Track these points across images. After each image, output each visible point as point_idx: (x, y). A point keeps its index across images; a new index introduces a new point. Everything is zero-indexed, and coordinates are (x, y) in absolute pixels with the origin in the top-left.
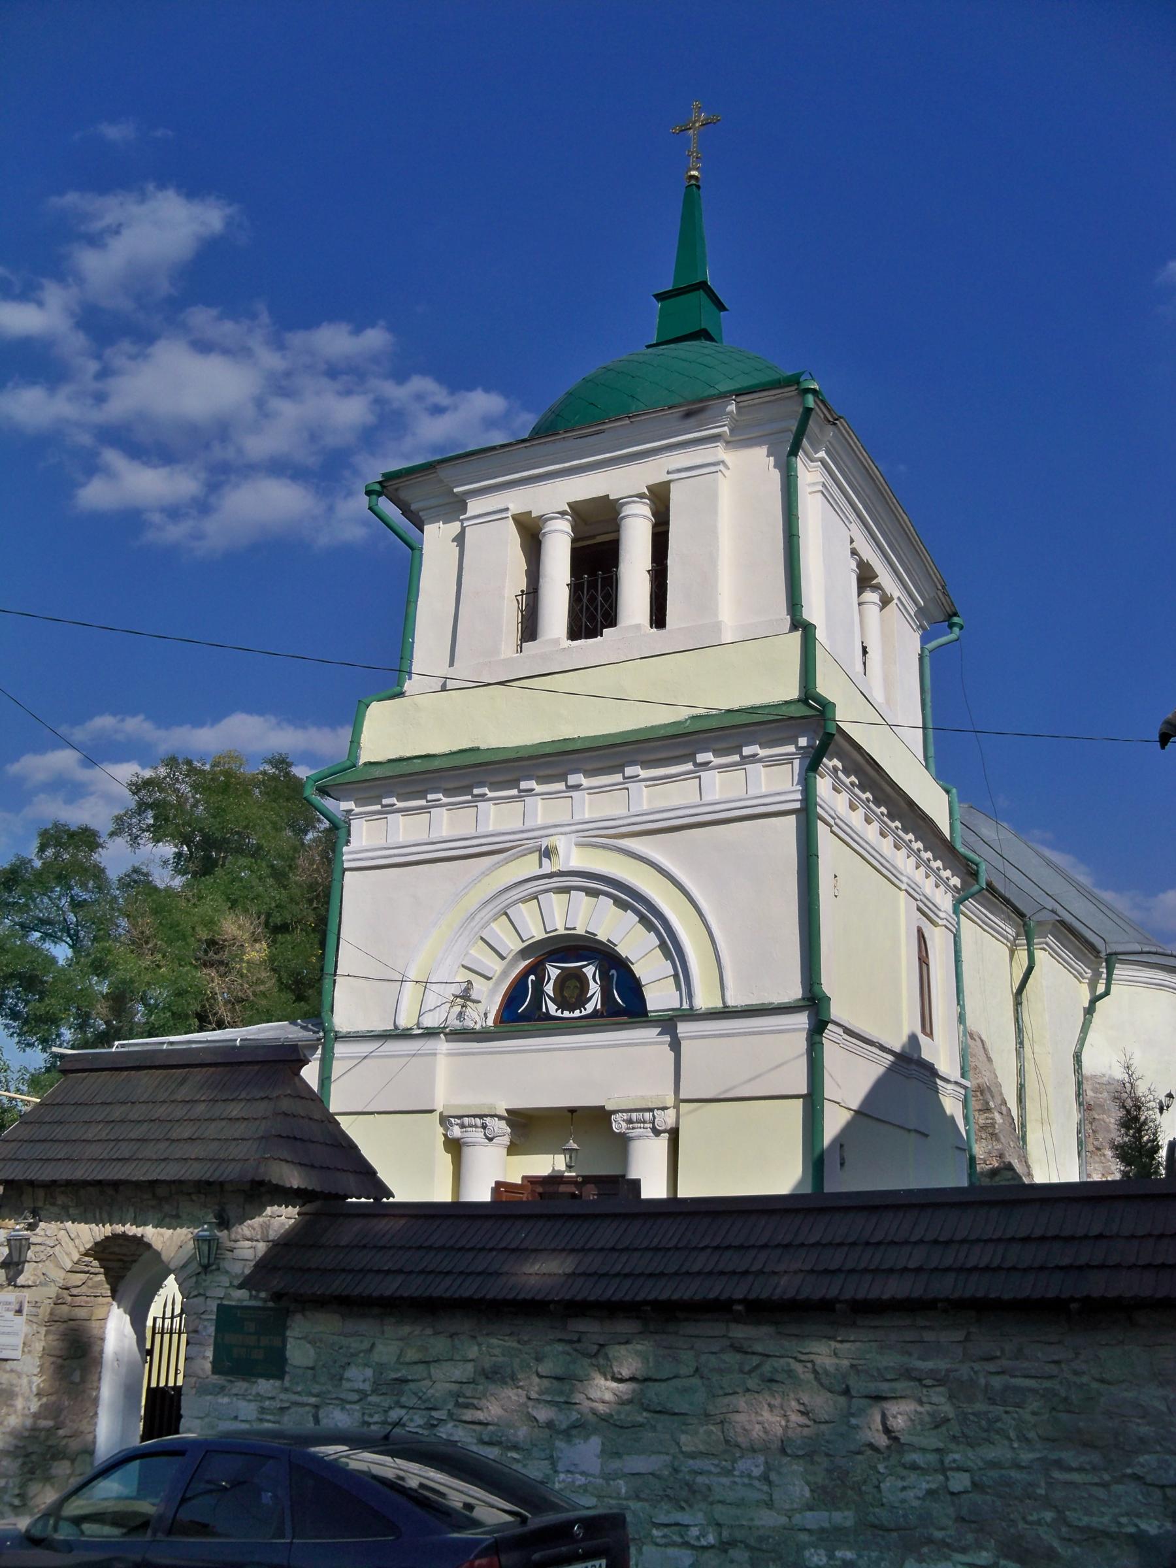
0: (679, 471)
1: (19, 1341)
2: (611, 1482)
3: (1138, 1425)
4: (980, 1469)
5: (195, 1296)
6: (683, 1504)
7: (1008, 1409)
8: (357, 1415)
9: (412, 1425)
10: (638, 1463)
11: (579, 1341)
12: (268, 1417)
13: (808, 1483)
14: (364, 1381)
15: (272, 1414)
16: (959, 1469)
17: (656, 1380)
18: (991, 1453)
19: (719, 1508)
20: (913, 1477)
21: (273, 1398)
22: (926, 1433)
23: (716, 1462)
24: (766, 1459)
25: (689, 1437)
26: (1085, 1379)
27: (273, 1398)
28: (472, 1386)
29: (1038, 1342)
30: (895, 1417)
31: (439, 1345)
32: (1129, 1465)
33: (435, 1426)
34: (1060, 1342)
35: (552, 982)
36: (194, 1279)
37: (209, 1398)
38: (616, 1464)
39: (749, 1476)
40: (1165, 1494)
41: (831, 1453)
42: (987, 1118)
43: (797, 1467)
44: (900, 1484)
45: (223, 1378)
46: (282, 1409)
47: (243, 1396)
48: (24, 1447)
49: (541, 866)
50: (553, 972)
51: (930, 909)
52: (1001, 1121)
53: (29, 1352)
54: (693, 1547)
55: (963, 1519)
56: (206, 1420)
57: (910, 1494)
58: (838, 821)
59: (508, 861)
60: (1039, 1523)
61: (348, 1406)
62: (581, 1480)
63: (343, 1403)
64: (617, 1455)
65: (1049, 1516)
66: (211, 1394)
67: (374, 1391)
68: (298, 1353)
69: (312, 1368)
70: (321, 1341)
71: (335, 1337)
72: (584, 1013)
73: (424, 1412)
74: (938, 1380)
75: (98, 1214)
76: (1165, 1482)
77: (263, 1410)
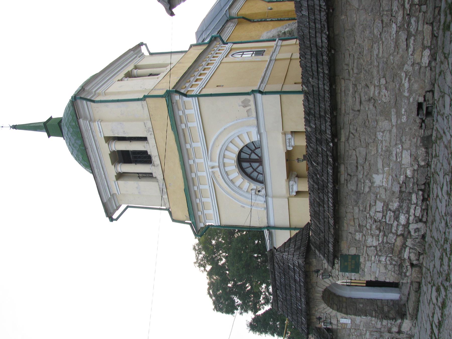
0: (101, 134)
2: (385, 172)
3: (366, 33)
4: (379, 76)
5: (338, 277)
6: (390, 153)
7: (363, 68)
8: (369, 236)
9: (371, 222)
10: (380, 165)
11: (347, 180)
12: (370, 259)
13: (384, 121)
14: (359, 235)
15: (369, 258)
16: (380, 82)
17: (357, 160)
18: (375, 73)
19: (391, 144)
20: (382, 94)
21: (365, 258)
22: (370, 90)
23: (379, 144)
24: (378, 132)
25: (372, 152)
26: (354, 47)
27: (365, 258)
28: (360, 207)
29: (344, 60)
30: (366, 98)
31: (349, 216)
32: (377, 36)
33: (371, 216)
34: (344, 54)
36: (334, 278)
37: (365, 274)
38: (380, 171)
39: (383, 136)
40: (385, 27)
41: (376, 115)
42: (287, 33)
43: (380, 123)
44: (384, 97)
45: (360, 270)
46: (368, 255)
47: (365, 265)
48: (380, 319)
51: (226, 53)
52: (288, 29)
54: (402, 150)
55: (393, 80)
56: (371, 274)
57: (386, 94)
58: (201, 86)
59: (216, 180)
60: (394, 60)
61: (366, 239)
62: (385, 180)
63: (365, 240)
64: (378, 170)
65: (391, 58)
67: (362, 232)
68: (353, 251)
69: (356, 248)
70: (349, 246)
71: (348, 242)
73: (367, 219)
74: (355, 87)
75: (317, 303)
76: (381, 27)
77: (368, 260)
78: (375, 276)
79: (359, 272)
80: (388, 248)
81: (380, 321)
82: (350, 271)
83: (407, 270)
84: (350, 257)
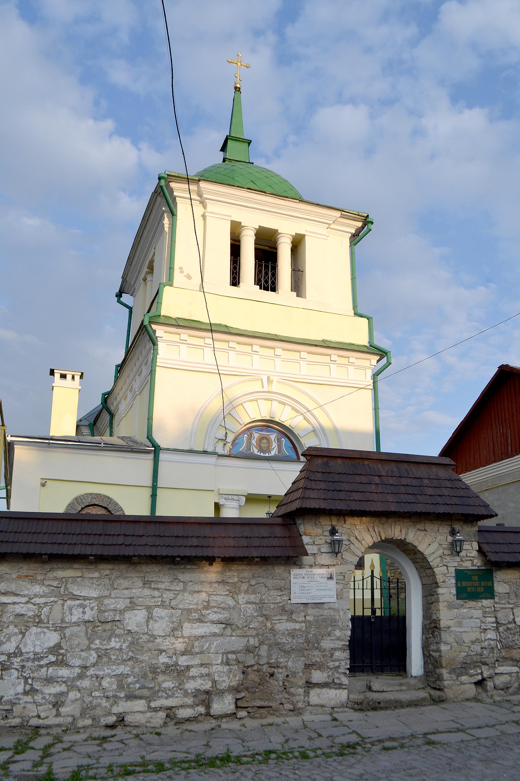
1: (334, 593)
15: (489, 613)
21: (490, 607)
35: (255, 439)
37: (455, 610)
45: (463, 601)
49: (263, 387)
50: (256, 435)
53: (341, 598)
59: (244, 381)
66: (456, 609)
68: (500, 588)
70: (511, 582)
72: (270, 455)
78: (453, 625)
79: (457, 599)
80: (514, 641)
81: (344, 645)
82: (459, 585)
83: (472, 676)
84: (490, 584)
